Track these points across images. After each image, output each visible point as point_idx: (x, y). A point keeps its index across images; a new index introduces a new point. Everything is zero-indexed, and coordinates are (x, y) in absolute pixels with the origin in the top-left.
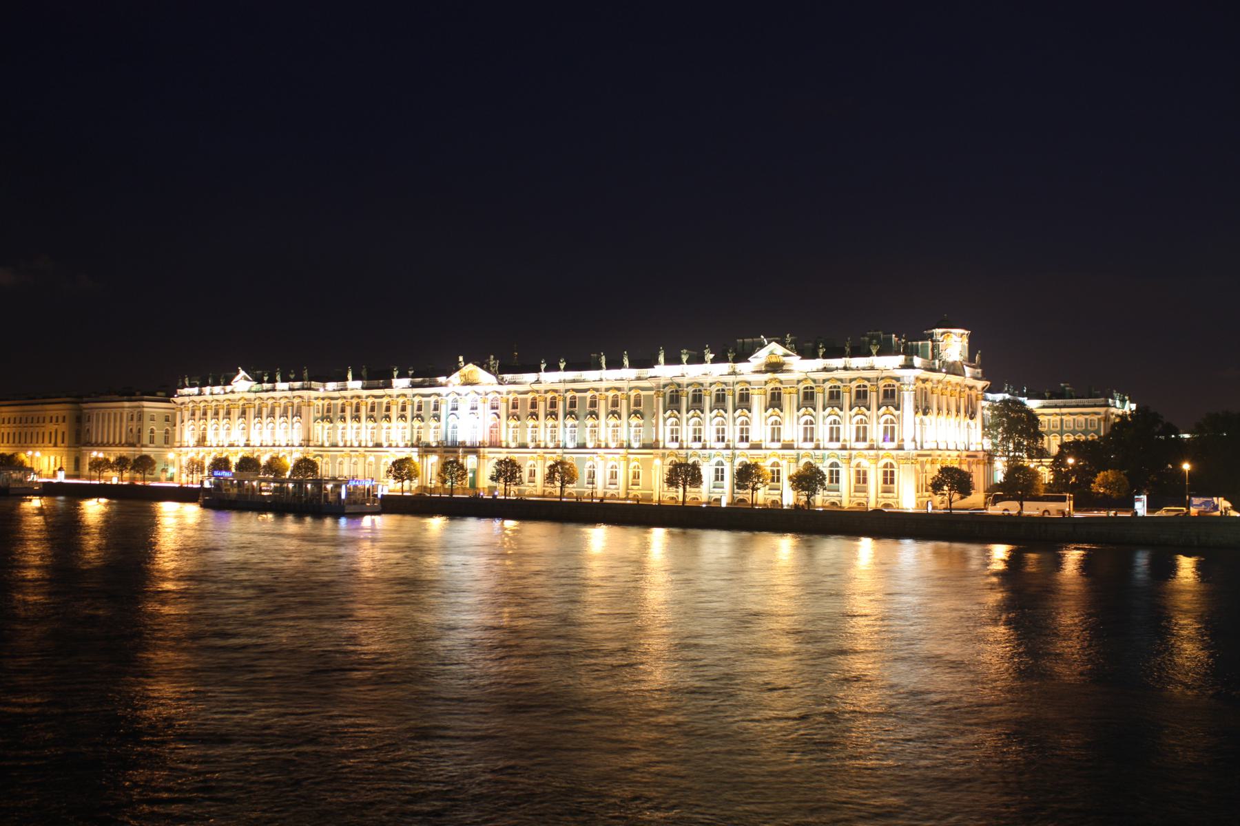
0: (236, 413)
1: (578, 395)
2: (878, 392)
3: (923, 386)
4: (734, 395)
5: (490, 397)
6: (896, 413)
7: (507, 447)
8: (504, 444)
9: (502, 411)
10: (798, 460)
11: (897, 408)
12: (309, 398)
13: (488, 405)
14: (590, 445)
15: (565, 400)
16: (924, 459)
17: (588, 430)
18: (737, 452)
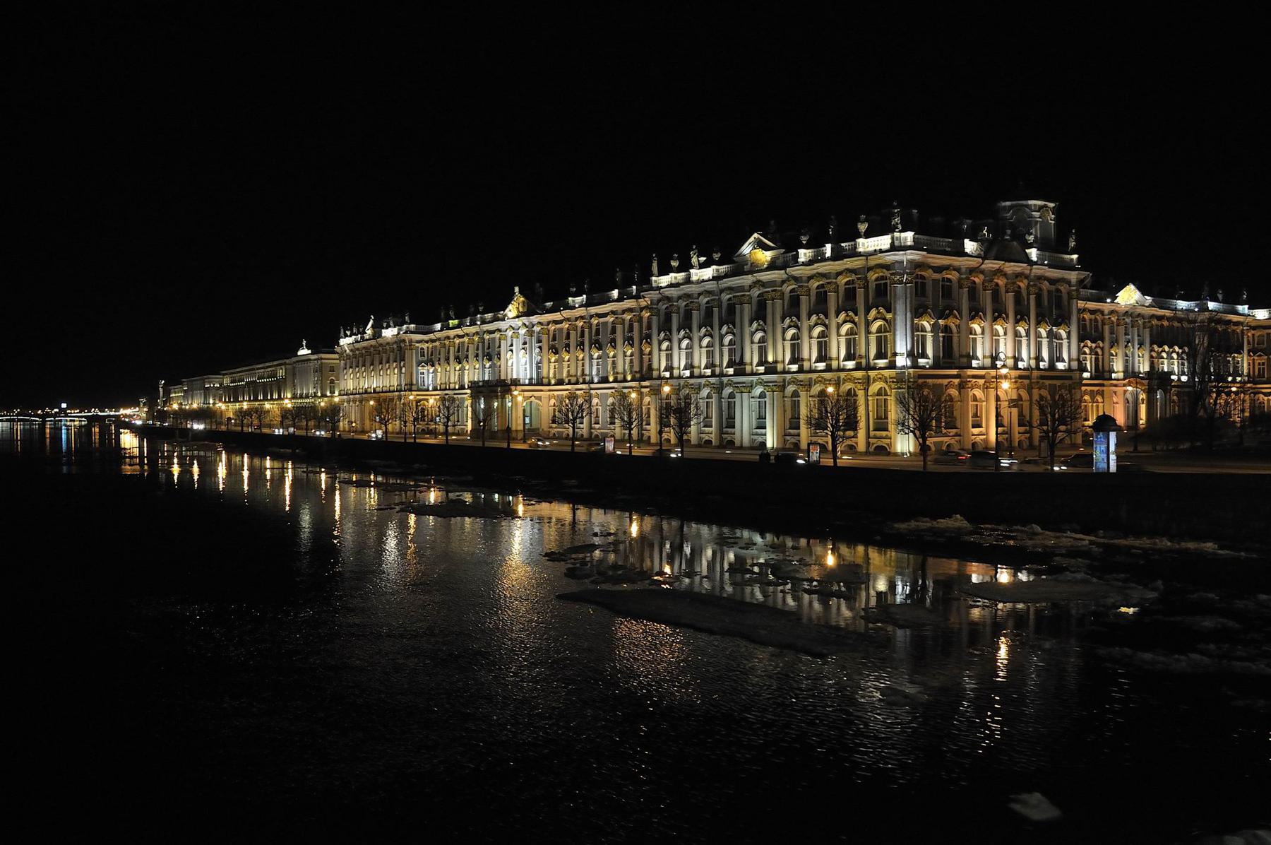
0: (368, 359)
1: (602, 320)
2: (866, 287)
3: (937, 276)
4: (720, 307)
5: (537, 329)
6: (889, 316)
7: (549, 384)
8: (545, 381)
9: (545, 346)
10: (783, 387)
11: (889, 311)
12: (411, 341)
13: (534, 339)
14: (611, 379)
15: (590, 328)
16: (945, 382)
17: (610, 360)
18: (725, 380)
